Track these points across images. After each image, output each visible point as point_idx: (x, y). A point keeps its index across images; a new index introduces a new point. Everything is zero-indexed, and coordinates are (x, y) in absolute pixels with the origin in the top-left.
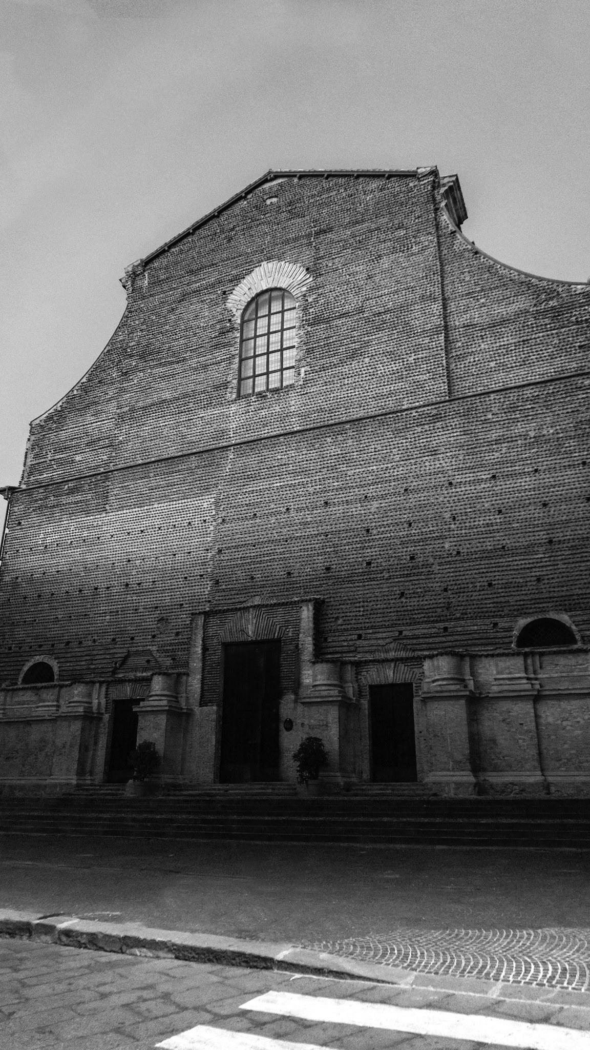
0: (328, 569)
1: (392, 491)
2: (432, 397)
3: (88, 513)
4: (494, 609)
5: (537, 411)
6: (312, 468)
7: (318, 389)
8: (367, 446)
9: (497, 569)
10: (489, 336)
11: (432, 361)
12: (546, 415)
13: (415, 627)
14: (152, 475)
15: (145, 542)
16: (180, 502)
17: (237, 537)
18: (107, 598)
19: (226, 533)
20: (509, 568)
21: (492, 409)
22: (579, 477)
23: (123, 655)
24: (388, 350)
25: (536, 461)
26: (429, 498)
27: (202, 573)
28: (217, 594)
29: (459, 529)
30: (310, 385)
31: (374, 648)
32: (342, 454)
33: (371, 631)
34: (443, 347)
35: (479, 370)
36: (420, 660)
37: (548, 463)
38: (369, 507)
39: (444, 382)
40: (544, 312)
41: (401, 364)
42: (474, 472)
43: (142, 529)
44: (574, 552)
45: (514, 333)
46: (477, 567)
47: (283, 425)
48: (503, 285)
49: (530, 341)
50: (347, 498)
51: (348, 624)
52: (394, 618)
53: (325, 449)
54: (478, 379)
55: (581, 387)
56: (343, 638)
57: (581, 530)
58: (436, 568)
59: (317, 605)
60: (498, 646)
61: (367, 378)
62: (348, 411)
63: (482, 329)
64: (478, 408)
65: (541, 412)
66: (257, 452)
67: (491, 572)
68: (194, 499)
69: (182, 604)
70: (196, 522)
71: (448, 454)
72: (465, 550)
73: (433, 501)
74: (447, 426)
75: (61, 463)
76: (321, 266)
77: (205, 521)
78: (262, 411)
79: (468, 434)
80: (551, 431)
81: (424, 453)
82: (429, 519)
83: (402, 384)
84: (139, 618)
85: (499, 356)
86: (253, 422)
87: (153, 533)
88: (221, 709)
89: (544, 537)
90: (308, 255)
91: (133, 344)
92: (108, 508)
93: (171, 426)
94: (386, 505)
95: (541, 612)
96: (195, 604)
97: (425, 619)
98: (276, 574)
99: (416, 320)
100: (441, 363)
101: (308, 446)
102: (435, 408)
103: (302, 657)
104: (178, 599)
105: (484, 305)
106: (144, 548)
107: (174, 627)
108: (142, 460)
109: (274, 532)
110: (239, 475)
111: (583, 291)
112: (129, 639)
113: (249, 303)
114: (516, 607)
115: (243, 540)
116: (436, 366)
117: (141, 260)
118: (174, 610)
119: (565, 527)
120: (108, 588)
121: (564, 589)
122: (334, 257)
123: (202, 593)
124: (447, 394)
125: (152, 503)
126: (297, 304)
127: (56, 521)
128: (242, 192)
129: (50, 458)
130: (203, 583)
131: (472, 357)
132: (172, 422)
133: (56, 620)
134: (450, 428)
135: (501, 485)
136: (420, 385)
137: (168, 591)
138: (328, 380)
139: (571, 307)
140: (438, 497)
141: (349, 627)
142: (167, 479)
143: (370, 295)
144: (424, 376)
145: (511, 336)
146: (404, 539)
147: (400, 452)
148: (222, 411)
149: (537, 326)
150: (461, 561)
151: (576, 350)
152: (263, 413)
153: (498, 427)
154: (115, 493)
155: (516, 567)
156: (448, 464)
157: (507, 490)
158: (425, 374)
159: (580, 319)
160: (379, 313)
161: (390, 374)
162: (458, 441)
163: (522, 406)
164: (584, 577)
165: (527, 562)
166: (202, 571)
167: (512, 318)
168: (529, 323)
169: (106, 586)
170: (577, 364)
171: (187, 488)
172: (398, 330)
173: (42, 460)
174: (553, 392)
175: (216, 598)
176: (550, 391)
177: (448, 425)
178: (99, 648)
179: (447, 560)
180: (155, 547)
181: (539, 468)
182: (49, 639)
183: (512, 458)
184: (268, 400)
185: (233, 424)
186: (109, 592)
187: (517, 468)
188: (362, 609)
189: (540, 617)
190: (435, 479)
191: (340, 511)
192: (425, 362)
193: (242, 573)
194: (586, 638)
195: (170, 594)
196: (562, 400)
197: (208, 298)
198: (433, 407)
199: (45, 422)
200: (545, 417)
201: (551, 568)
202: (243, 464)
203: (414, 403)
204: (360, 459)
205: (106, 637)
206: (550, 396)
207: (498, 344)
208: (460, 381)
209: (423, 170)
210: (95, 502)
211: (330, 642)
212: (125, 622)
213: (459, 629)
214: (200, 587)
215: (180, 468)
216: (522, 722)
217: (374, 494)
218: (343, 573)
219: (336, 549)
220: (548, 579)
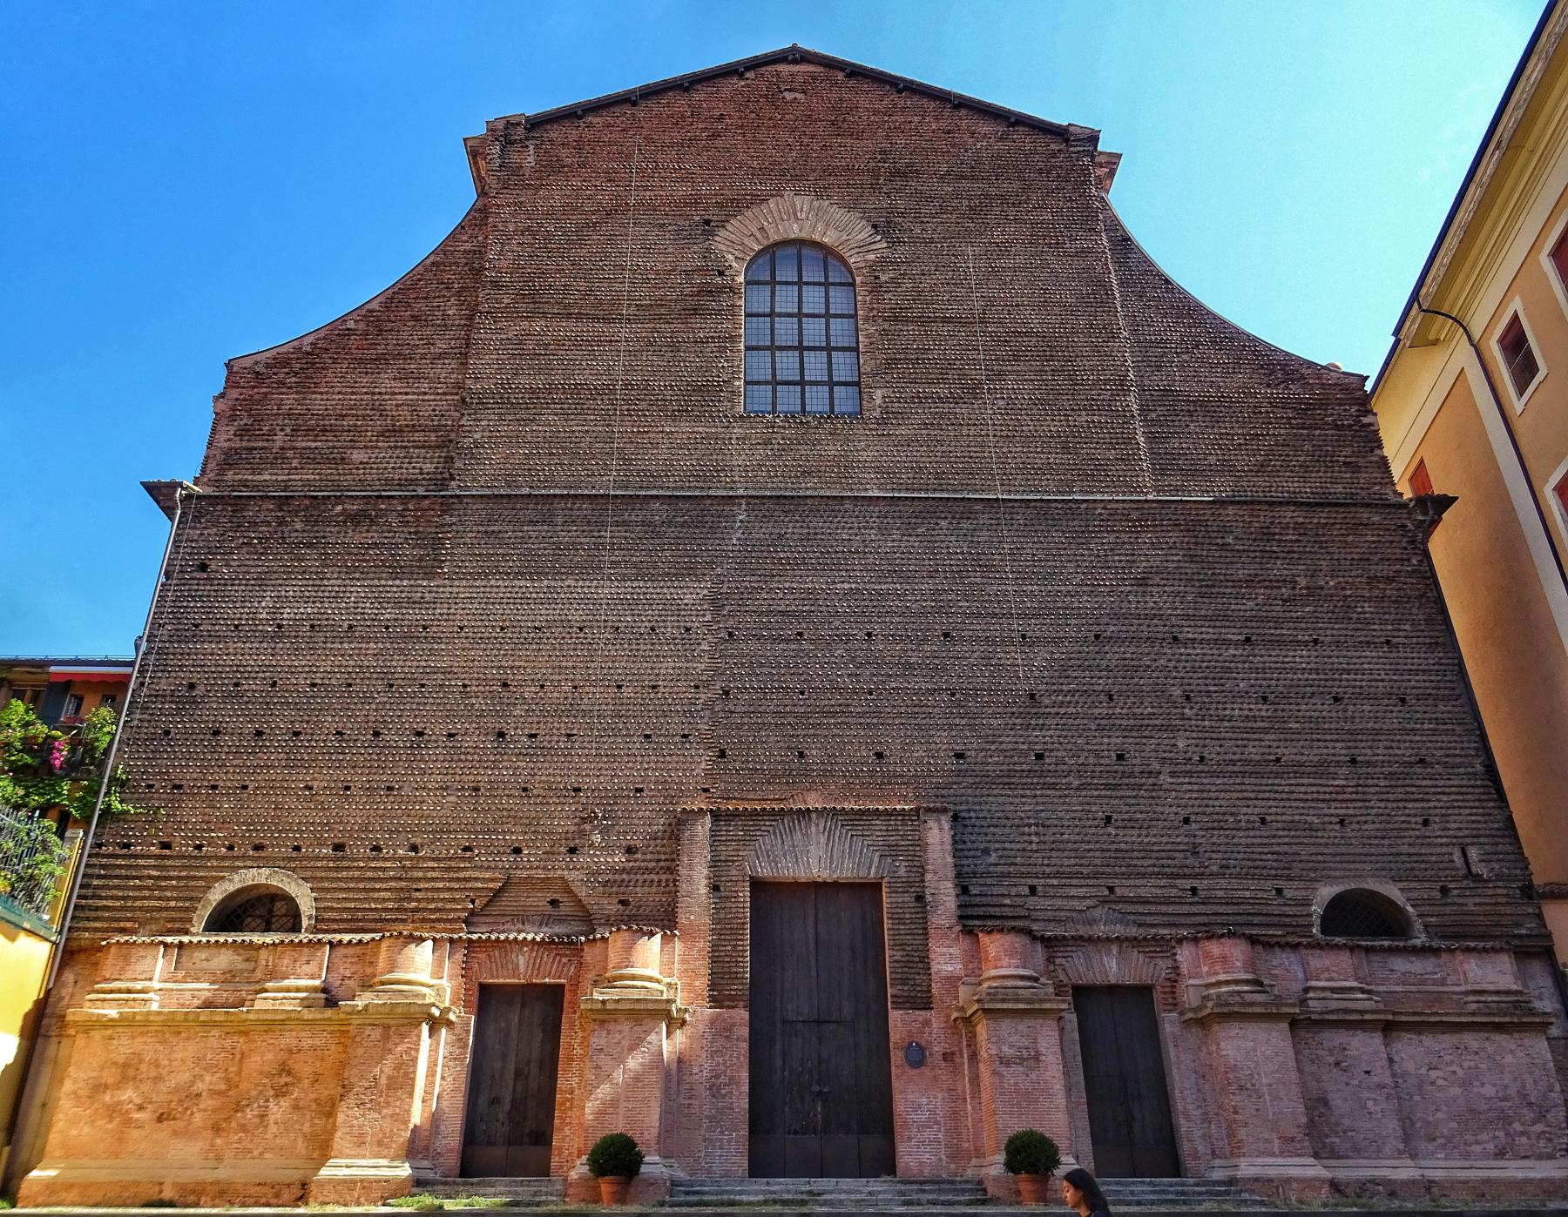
0: (959, 756)
9: (1273, 795)
13: (1138, 882)
31: (1063, 914)
33: (1055, 882)
36: (1164, 946)
42: (1215, 627)
44: (1393, 783)
51: (1010, 865)
56: (1002, 890)
57: (1399, 748)
60: (1290, 929)
67: (1263, 799)
73: (1148, 663)
77: (687, 630)
80: (1332, 583)
89: (1343, 752)
95: (1355, 876)
97: (1156, 869)
103: (933, 920)
108: (531, 487)
119: (1374, 741)
121: (1386, 842)
150: (1213, 774)
155: (1302, 796)
165: (1320, 789)
173: (260, 444)
180: (570, 664)
181: (1321, 639)
187: (1284, 632)
188: (1034, 839)
189: (1353, 886)
190: (1149, 626)
199: (267, 366)
209: (1080, 131)
211: (975, 895)
213: (1220, 894)
216: (1369, 1069)
218: (989, 767)
220: (1358, 823)
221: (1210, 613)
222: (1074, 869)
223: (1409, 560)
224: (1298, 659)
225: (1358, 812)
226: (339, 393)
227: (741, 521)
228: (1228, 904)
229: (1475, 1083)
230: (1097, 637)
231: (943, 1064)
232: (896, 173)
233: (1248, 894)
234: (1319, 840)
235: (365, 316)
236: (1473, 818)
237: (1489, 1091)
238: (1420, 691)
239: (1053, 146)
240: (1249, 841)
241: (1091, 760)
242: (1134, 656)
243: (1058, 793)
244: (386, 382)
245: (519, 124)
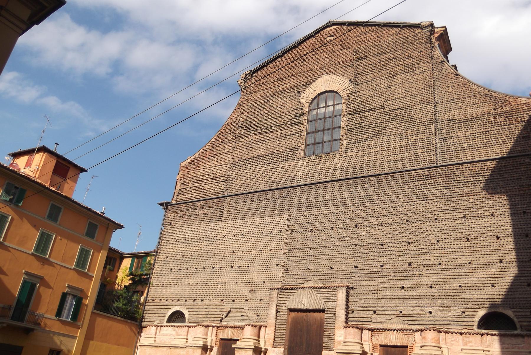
0: (356, 267)
1: (399, 221)
2: (425, 163)
3: (211, 221)
4: (462, 303)
5: (494, 177)
6: (348, 203)
7: (353, 154)
8: (383, 192)
10: (463, 127)
11: (426, 141)
12: (500, 180)
14: (250, 200)
15: (244, 242)
16: (266, 218)
18: (219, 274)
19: (293, 240)
20: (473, 277)
21: (464, 174)
22: (520, 221)
24: (399, 133)
25: (492, 209)
26: (421, 227)
27: (277, 264)
29: (441, 248)
30: (349, 151)
32: (367, 196)
34: (433, 133)
35: (456, 148)
37: (501, 210)
38: (383, 230)
39: (434, 155)
40: (500, 114)
41: (407, 141)
43: (243, 233)
45: (480, 126)
46: (452, 274)
47: (331, 175)
48: (474, 96)
49: (490, 132)
50: (369, 224)
52: (397, 302)
53: (357, 192)
54: (455, 154)
55: (523, 163)
56: (364, 312)
57: (521, 256)
58: (424, 272)
59: (348, 290)
60: (465, 327)
61: (384, 149)
62: (372, 169)
63: (459, 123)
64: (455, 173)
65: (496, 178)
66: (315, 191)
68: (275, 217)
69: (264, 282)
70: (275, 231)
71: (434, 200)
72: (444, 262)
73: (424, 229)
74: (434, 183)
75: (196, 189)
76: (358, 79)
77: (281, 231)
78: (319, 165)
79: (448, 189)
81: (419, 199)
82: (421, 241)
83: (407, 154)
84: (238, 288)
85: (470, 140)
86: (313, 172)
87: (249, 236)
88: (287, 350)
90: (351, 71)
92: (223, 218)
93: (263, 171)
94: (394, 229)
96: (272, 283)
97: (417, 305)
98: (323, 268)
99: (417, 115)
100: (432, 143)
101: (346, 189)
102: (427, 171)
104: (262, 279)
105: (460, 108)
106: (243, 245)
107: (259, 296)
109: (323, 241)
110: (303, 204)
111: (526, 102)
113: (314, 99)
114: (476, 303)
115: (303, 245)
116: (429, 144)
117: (251, 71)
118: (259, 285)
120: (220, 268)
122: (367, 74)
123: (277, 276)
124: (435, 162)
125: (249, 218)
126: (343, 101)
127: (192, 224)
128: (312, 33)
129: (190, 186)
130: (278, 270)
131: (452, 139)
132: (264, 169)
133: (189, 285)
134: (436, 184)
135: (469, 223)
136: (418, 155)
137: (256, 273)
138: (360, 149)
139: (518, 111)
140: (427, 227)
141: (368, 305)
142: (259, 203)
143: (389, 98)
144: (421, 150)
145: (478, 128)
146: (405, 252)
147: (404, 197)
148: (294, 164)
149: (495, 123)
150: (442, 269)
151: (520, 139)
152: (320, 166)
153: (467, 185)
154: (228, 210)
156: (434, 207)
157: (473, 226)
158: (422, 149)
159: (523, 120)
160: (394, 109)
161: (399, 148)
162: (442, 193)
163: (484, 173)
164: (523, 287)
165: (485, 273)
166: (278, 262)
167: (479, 116)
168: (490, 120)
169: (219, 267)
170: (521, 148)
171: (271, 210)
172: (405, 121)
173: (186, 187)
174: (505, 166)
175: (286, 280)
176: (503, 165)
177: (435, 182)
178: (213, 304)
179: (432, 268)
180: (250, 245)
181: (494, 213)
182: (184, 297)
183: (476, 206)
184: (322, 159)
185: (300, 172)
186: (221, 270)
188: (376, 295)
191: (364, 232)
192: (421, 142)
194: (523, 327)
195: (257, 275)
196: (510, 171)
197: (289, 95)
198: (426, 170)
200: (499, 181)
202: (305, 198)
203: (414, 166)
204: (379, 199)
205: (218, 298)
206: (503, 168)
207: (469, 133)
208: (444, 154)
210: (216, 214)
212: (230, 290)
213: (439, 313)
214: (276, 272)
215: (267, 197)
217: (387, 222)
219: (362, 255)
222: (388, 305)
225: (499, 282)
233: (450, 314)
234: (482, 293)
239: (417, 32)
240: (454, 294)
242: (419, 227)
245: (249, 73)
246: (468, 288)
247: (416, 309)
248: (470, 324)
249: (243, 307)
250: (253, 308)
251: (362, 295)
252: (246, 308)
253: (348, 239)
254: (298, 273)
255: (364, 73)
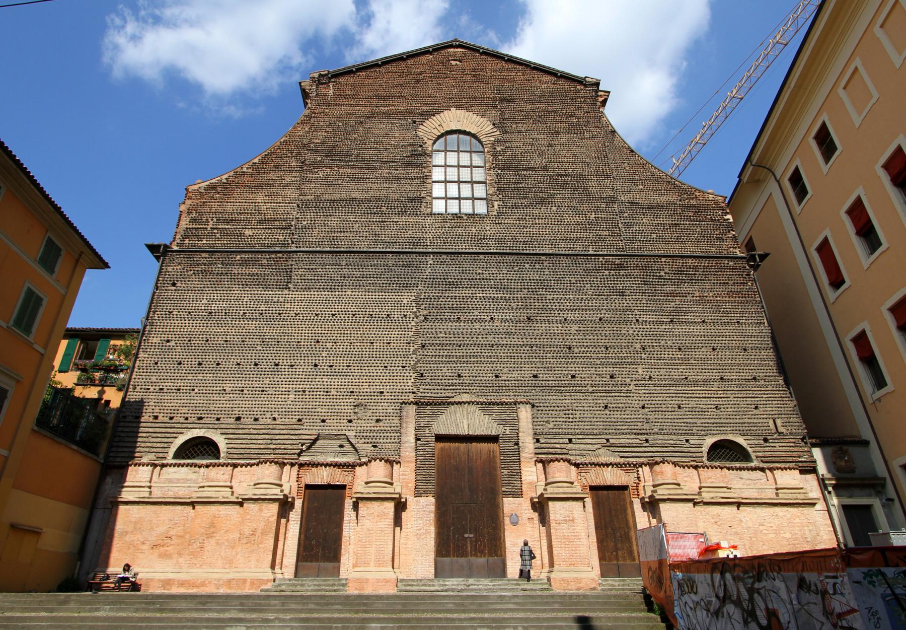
0: (535, 376)
9: (683, 395)
17: (442, 335)
20: (693, 396)
23: (313, 437)
27: (404, 365)
28: (424, 387)
33: (581, 437)
38: (569, 328)
46: (668, 391)
50: (548, 318)
57: (743, 373)
58: (632, 388)
60: (692, 459)
67: (679, 397)
69: (382, 392)
70: (396, 315)
72: (655, 376)
73: (625, 332)
77: (405, 316)
89: (717, 374)
91: (317, 141)
97: (629, 431)
98: (484, 375)
103: (523, 455)
112: (320, 421)
113: (439, 137)
135: (678, 329)
136: (602, 239)
139: (707, 208)
150: (655, 385)
165: (706, 392)
169: (290, 364)
175: (422, 390)
181: (706, 320)
188: (571, 416)
193: (448, 370)
201: (726, 399)
209: (591, 80)
213: (659, 442)
218: (550, 382)
221: (654, 308)
223: (747, 283)
224: (695, 330)
225: (724, 403)
226: (239, 202)
227: (431, 264)
228: (663, 447)
229: (782, 532)
230: (600, 320)
231: (528, 524)
232: (502, 100)
233: (672, 442)
234: (706, 416)
235: (252, 166)
236: (779, 405)
237: (788, 535)
238: (754, 345)
239: (578, 87)
240: (673, 417)
241: (598, 379)
243: (581, 394)
244: (260, 198)
245: (326, 75)
246: (690, 409)
247: (628, 436)
248: (698, 455)
249: (344, 432)
250: (365, 434)
251: (550, 416)
252: (351, 434)
253: (518, 337)
254: (442, 381)
255: (513, 119)
